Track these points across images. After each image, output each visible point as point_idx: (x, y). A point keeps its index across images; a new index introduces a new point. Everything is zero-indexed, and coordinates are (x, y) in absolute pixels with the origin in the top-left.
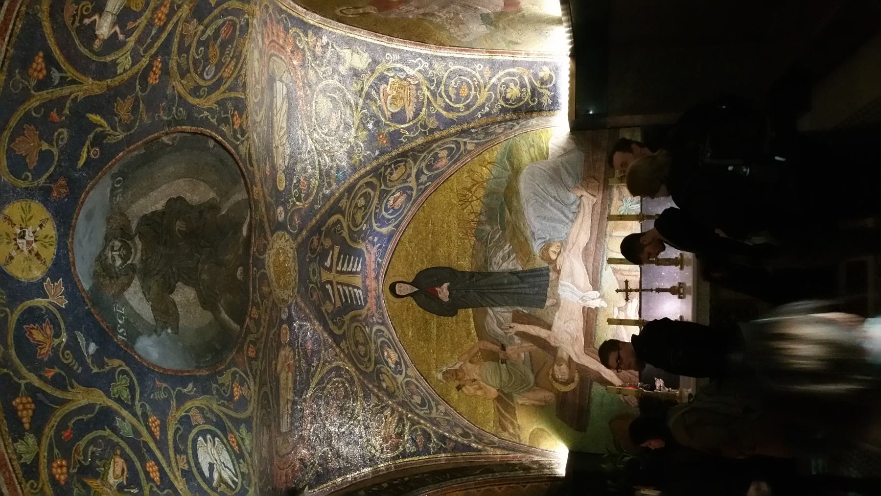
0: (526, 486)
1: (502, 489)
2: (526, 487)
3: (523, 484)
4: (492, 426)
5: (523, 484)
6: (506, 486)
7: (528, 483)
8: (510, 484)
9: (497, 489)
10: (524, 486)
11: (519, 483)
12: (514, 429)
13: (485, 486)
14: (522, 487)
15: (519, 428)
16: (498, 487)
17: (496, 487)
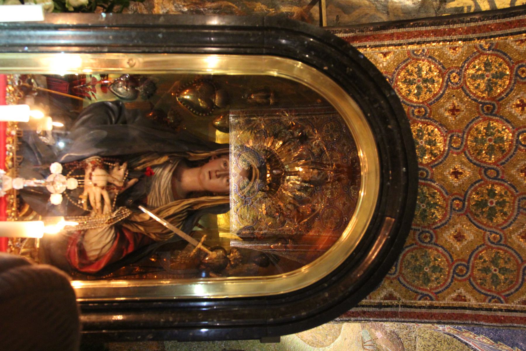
0: (385, 298)
1: (454, 295)
2: (384, 293)
3: (395, 302)
4: (419, 340)
5: (395, 302)
6: (442, 303)
7: (380, 306)
8: (431, 307)
9: (468, 297)
10: (391, 297)
11: (405, 306)
12: (374, 340)
13: (508, 310)
14: (396, 294)
15: (364, 343)
16: (466, 304)
17: (473, 303)
